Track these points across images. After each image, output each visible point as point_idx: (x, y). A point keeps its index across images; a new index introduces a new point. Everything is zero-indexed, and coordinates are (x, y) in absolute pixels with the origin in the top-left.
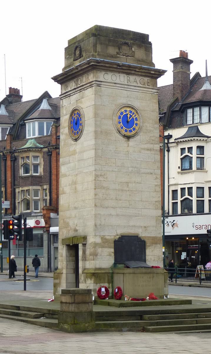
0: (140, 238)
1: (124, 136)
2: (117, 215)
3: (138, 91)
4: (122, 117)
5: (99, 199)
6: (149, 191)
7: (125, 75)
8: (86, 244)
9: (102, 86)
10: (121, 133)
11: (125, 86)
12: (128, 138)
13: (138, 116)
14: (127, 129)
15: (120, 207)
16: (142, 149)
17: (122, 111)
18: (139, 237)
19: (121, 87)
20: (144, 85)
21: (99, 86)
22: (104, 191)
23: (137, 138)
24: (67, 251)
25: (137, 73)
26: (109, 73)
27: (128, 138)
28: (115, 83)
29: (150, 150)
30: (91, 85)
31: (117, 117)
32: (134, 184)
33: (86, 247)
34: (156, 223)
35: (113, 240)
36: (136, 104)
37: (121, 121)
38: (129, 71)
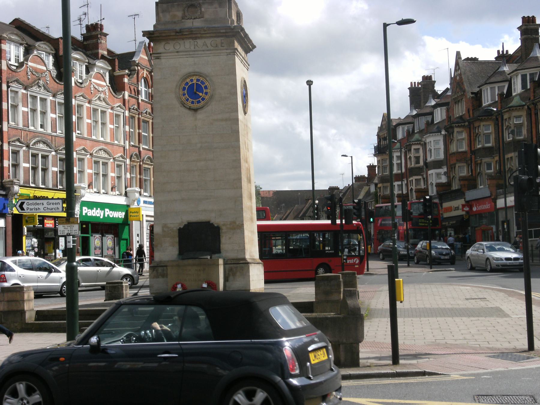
1: (190, 109)
3: (207, 55)
7: (191, 40)
10: (185, 105)
11: (191, 53)
12: (196, 110)
18: (211, 223)
19: (185, 55)
20: (217, 46)
23: (208, 109)
25: (204, 35)
26: (170, 42)
28: (177, 52)
29: (226, 120)
31: (181, 88)
35: (178, 228)
37: (186, 93)
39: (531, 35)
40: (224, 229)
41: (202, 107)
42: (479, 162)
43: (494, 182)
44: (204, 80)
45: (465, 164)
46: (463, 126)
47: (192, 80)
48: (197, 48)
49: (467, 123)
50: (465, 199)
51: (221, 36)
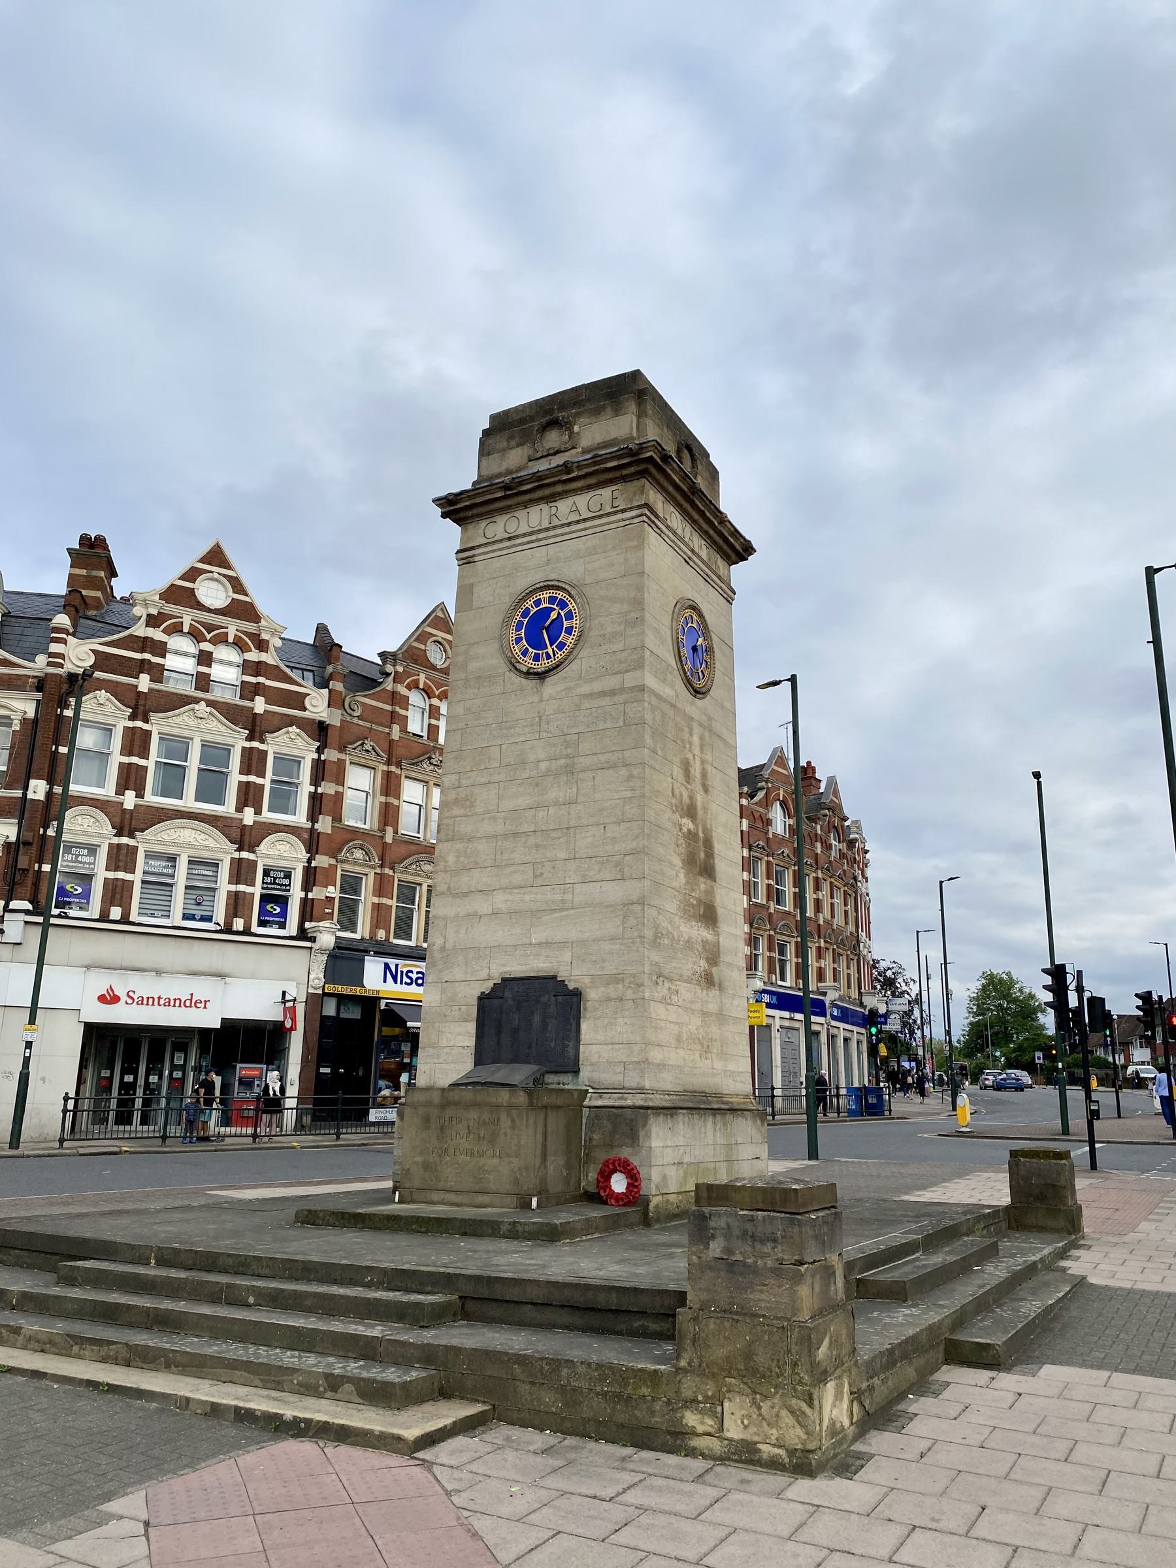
1: (529, 674)
2: (495, 914)
3: (579, 534)
9: (477, 559)
10: (517, 665)
12: (541, 676)
15: (505, 889)
16: (585, 696)
19: (528, 543)
22: (459, 846)
28: (510, 539)
29: (612, 693)
34: (624, 928)
36: (571, 572)
37: (523, 635)
38: (547, 492)
40: (592, 995)
41: (558, 666)
44: (566, 598)
47: (537, 603)
48: (556, 522)
51: (611, 482)
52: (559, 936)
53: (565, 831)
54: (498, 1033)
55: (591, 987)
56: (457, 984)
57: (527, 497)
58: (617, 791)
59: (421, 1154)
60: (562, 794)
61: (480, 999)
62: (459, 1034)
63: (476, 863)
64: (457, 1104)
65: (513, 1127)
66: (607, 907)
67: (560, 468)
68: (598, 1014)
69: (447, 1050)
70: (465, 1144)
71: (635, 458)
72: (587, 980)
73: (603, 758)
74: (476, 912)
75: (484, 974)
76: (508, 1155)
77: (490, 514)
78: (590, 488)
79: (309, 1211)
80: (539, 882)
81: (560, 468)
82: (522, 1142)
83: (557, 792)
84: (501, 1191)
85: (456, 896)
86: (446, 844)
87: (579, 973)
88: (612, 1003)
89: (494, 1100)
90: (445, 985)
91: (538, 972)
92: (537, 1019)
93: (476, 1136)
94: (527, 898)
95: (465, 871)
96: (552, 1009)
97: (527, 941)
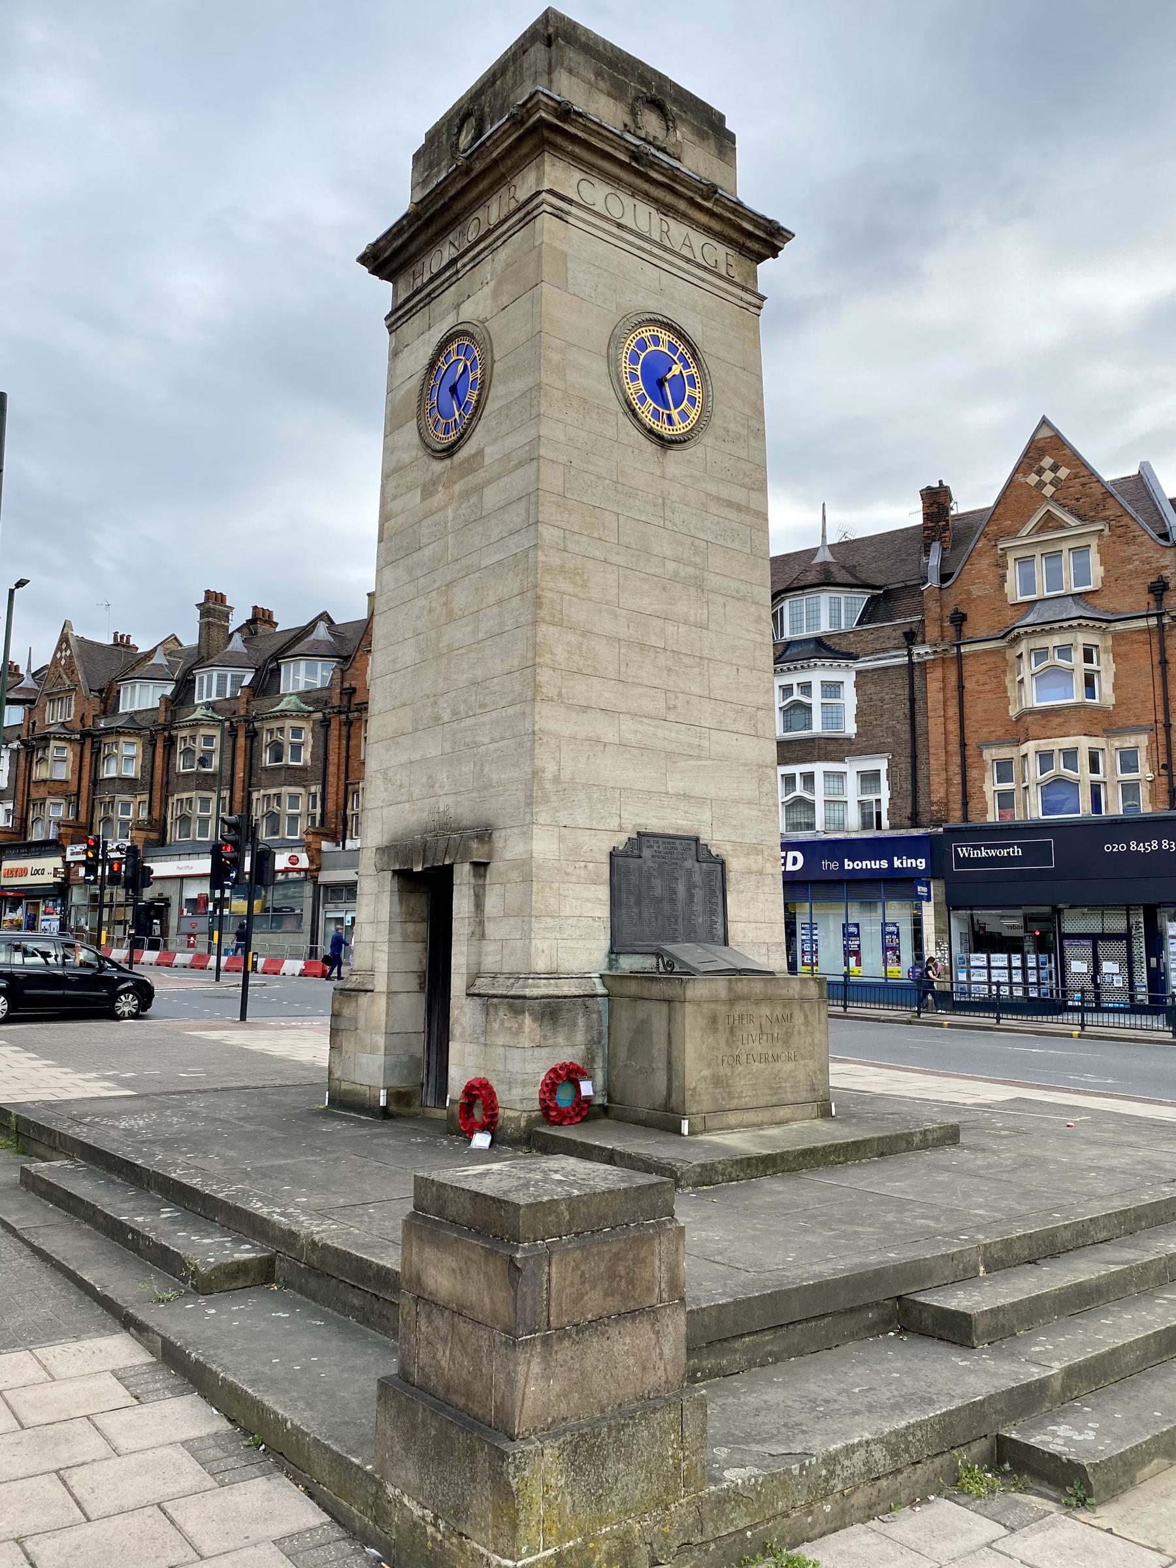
0: (707, 845)
2: (623, 745)
3: (695, 281)
4: (642, 358)
5: (554, 669)
6: (734, 662)
8: (489, 863)
13: (696, 370)
14: (661, 410)
15: (634, 715)
17: (643, 335)
19: (640, 248)
21: (561, 218)
22: (571, 637)
23: (693, 452)
24: (396, 898)
27: (665, 443)
28: (620, 226)
30: (528, 213)
32: (683, 629)
33: (485, 876)
34: (760, 792)
37: (639, 373)
38: (669, 198)
39: (220, 620)
42: (107, 800)
43: (142, 834)
45: (63, 801)
46: (69, 740)
49: (78, 737)
50: (64, 857)
52: (698, 789)
53: (698, 660)
54: (638, 903)
55: (732, 856)
56: (580, 831)
57: (646, 186)
58: (748, 631)
59: (709, 1065)
60: (692, 612)
61: (613, 855)
62: (588, 900)
63: (595, 669)
64: (746, 998)
65: (807, 1022)
66: (745, 765)
67: (702, 186)
68: (742, 887)
69: (573, 921)
70: (758, 1048)
71: (768, 238)
72: (728, 847)
73: (735, 585)
74: (598, 737)
75: (614, 823)
76: (803, 1058)
77: (589, 168)
78: (708, 230)
79: (703, 1166)
80: (671, 717)
81: (702, 186)
82: (816, 1041)
83: (686, 607)
84: (800, 1100)
85: (570, 707)
86: (551, 628)
87: (720, 838)
88: (753, 877)
89: (785, 991)
90: (566, 831)
91: (678, 829)
92: (681, 888)
93: (770, 1037)
94: (660, 732)
95: (580, 676)
96: (697, 878)
97: (663, 789)
